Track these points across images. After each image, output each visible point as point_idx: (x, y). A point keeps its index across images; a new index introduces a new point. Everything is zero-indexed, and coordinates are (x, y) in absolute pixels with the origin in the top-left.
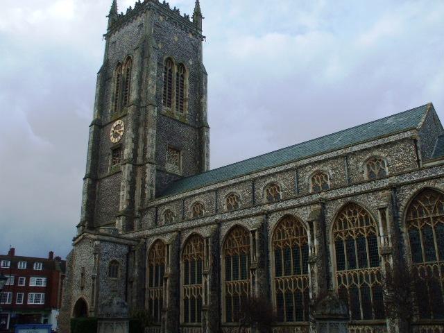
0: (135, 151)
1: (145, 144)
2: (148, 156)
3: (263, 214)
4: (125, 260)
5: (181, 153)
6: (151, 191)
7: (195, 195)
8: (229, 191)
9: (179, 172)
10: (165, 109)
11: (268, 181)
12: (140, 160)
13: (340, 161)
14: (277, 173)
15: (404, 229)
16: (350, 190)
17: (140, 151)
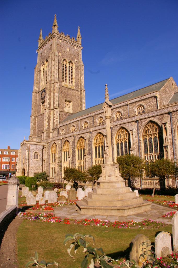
0: (50, 104)
1: (54, 100)
2: (55, 105)
5: (72, 102)
6: (57, 121)
8: (85, 121)
9: (71, 111)
10: (63, 83)
11: (99, 116)
12: (52, 108)
15: (142, 139)
16: (122, 121)
17: (52, 104)
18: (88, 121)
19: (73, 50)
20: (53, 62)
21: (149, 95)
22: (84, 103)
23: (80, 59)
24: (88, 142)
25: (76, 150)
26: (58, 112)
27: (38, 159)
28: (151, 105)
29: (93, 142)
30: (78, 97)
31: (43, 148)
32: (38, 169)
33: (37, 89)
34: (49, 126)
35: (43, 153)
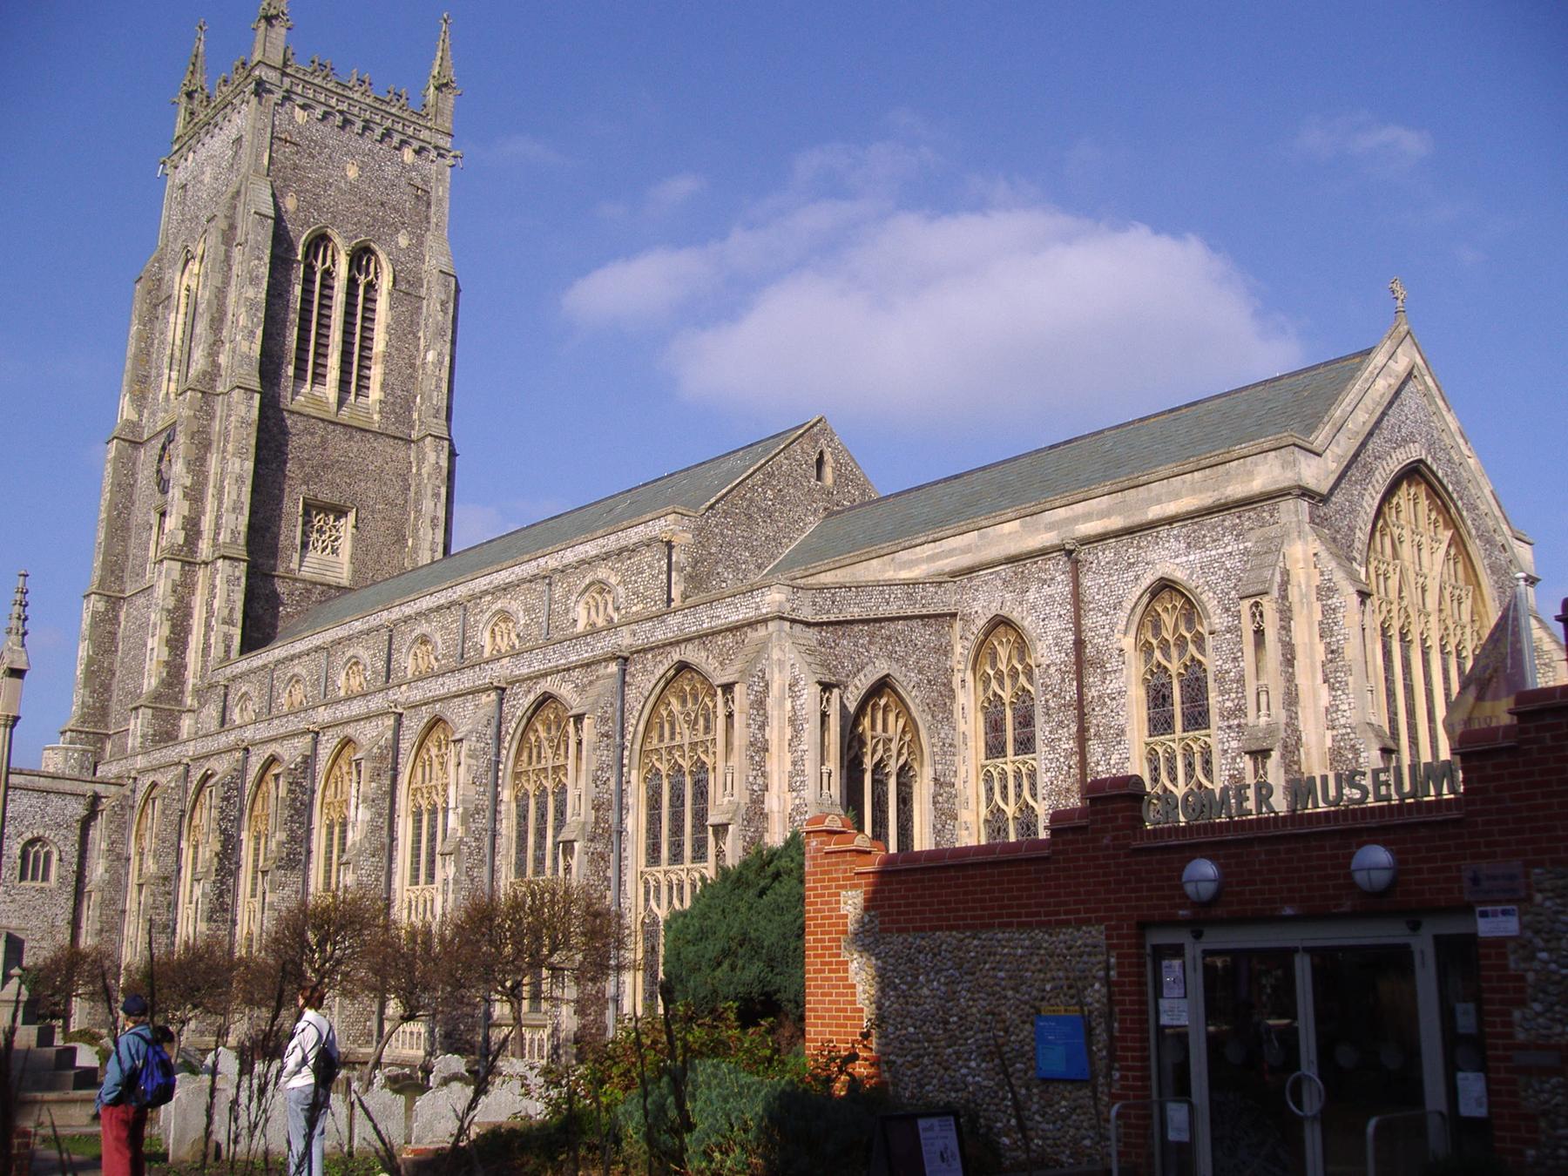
0: (192, 527)
1: (220, 502)
3: (309, 731)
4: (74, 837)
5: (352, 516)
6: (227, 638)
7: (292, 658)
12: (205, 548)
13: (541, 586)
14: (431, 610)
15: (506, 794)
17: (207, 523)
18: (365, 656)
19: (390, 171)
20: (236, 252)
21: (642, 527)
22: (434, 519)
23: (432, 226)
24: (290, 791)
25: (244, 835)
26: (243, 580)
28: (646, 589)
29: (318, 796)
30: (399, 484)
32: (44, 944)
33: (141, 416)
34: (175, 671)
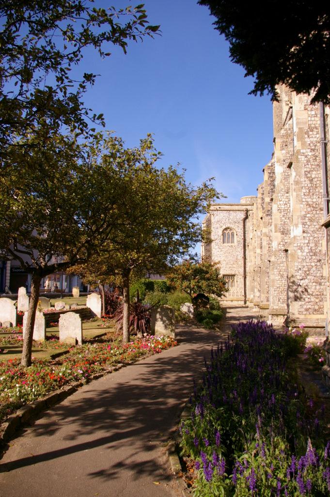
27: (232, 244)
31: (247, 218)
32: (234, 266)
35: (246, 229)
